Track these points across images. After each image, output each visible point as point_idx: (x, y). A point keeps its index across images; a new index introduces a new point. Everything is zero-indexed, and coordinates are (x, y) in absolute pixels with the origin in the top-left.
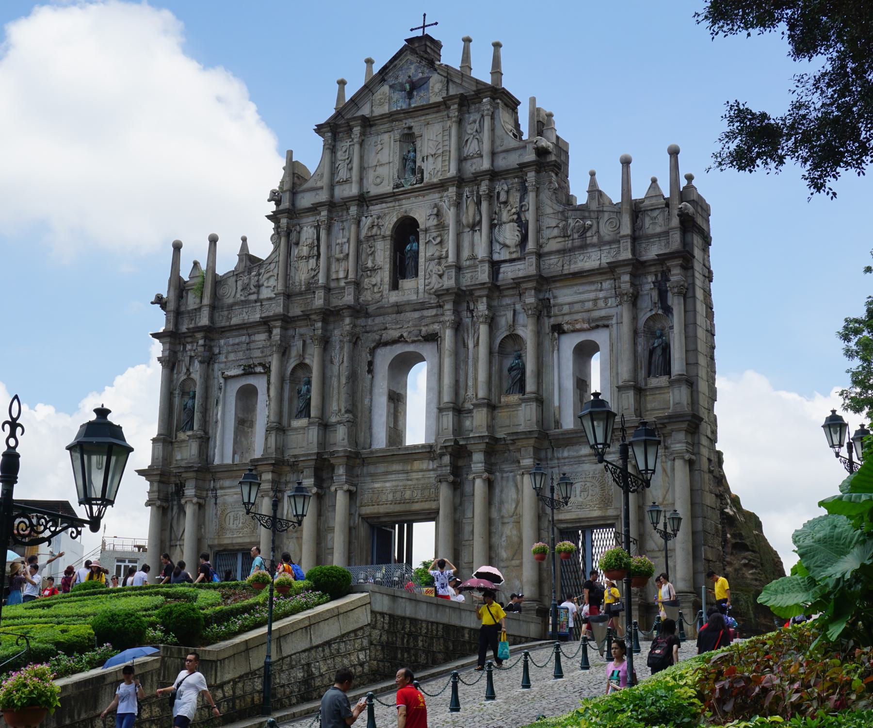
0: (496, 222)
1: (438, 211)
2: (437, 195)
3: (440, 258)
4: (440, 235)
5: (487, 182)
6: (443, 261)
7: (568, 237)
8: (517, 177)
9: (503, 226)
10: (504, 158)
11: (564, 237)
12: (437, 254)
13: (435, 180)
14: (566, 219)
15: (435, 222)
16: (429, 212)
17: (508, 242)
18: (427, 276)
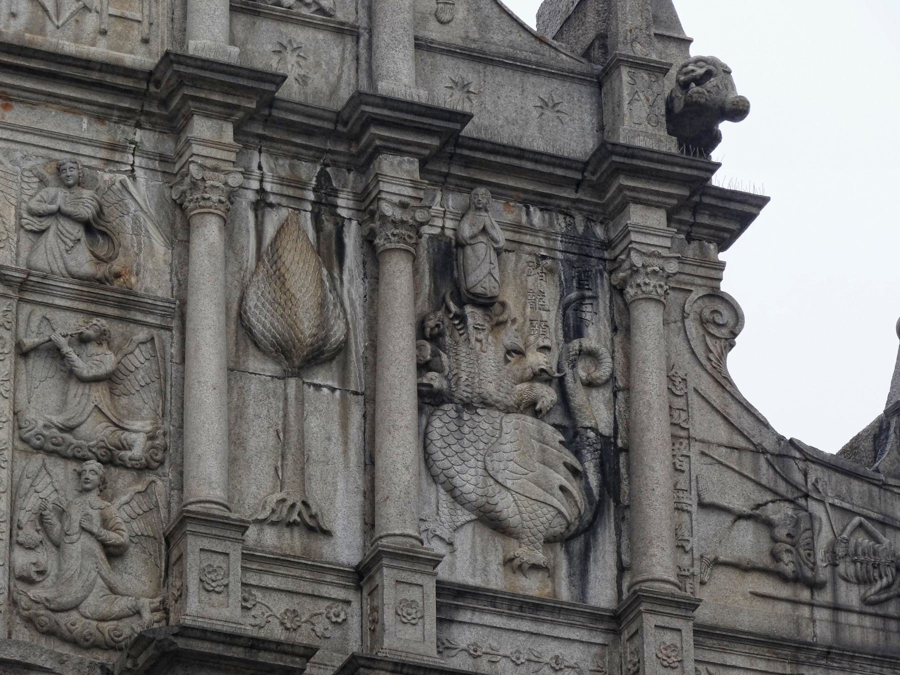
0: (435, 380)
1: (100, 213)
2: (84, 127)
3: (111, 459)
4: (102, 338)
5: (409, 167)
6: (126, 485)
7: (814, 586)
8: (545, 204)
9: (485, 420)
10: (465, 87)
11: (796, 580)
12: (95, 431)
13: (69, 47)
14: (799, 497)
15: (82, 261)
16: (60, 198)
17: (507, 506)
18: (29, 533)
